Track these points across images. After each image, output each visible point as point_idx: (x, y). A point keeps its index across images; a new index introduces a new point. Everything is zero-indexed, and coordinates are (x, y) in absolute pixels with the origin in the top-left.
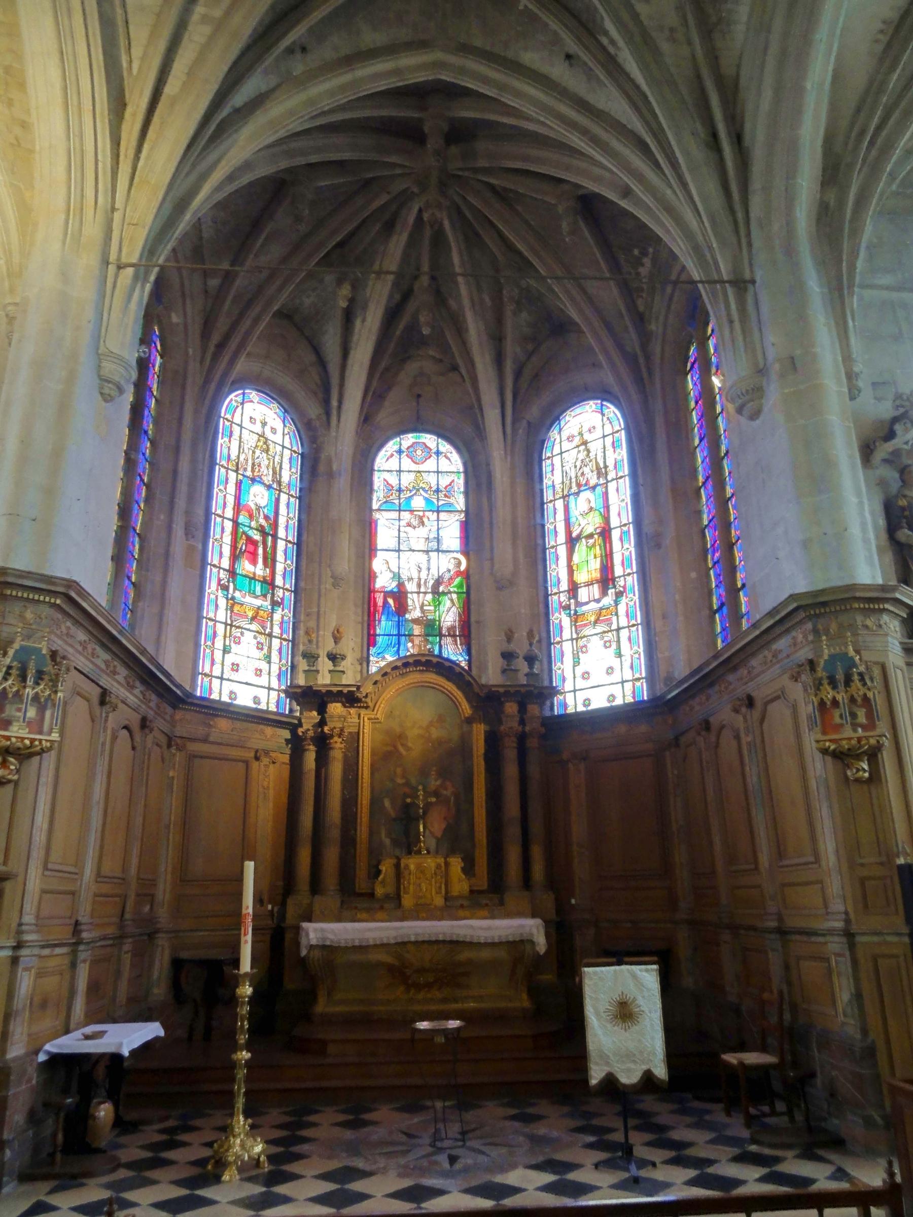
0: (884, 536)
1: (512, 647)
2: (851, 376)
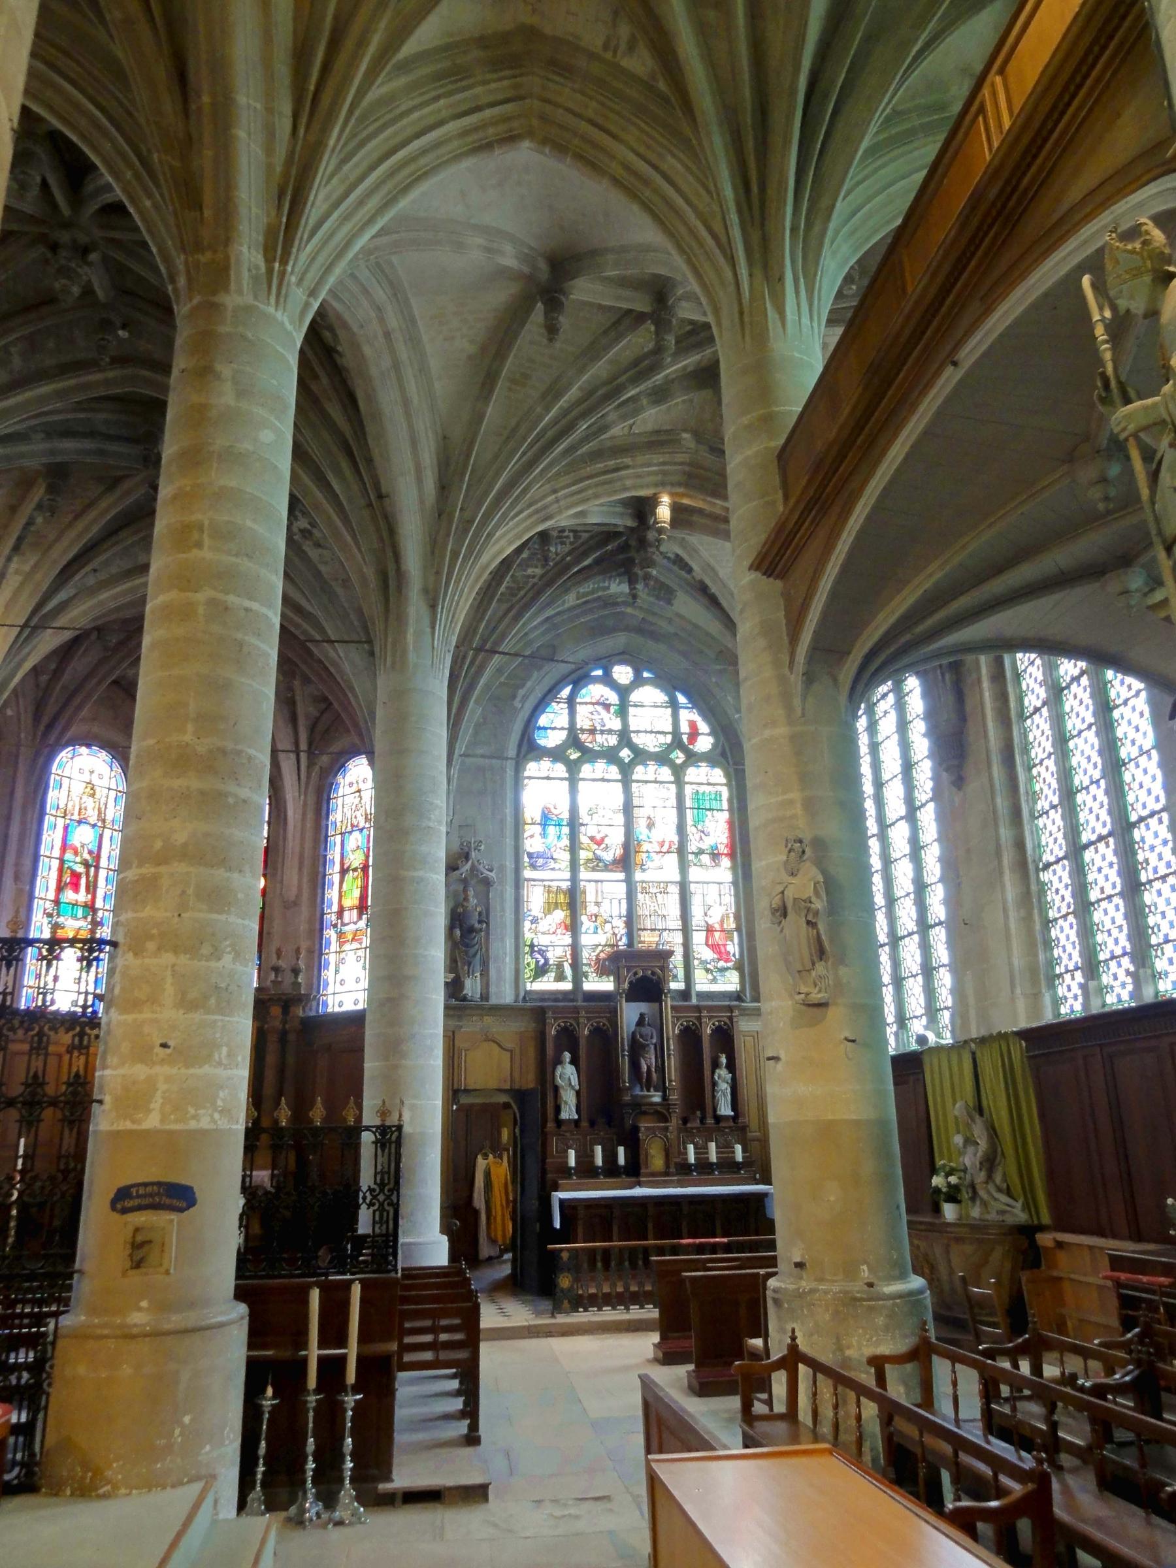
1: (281, 963)
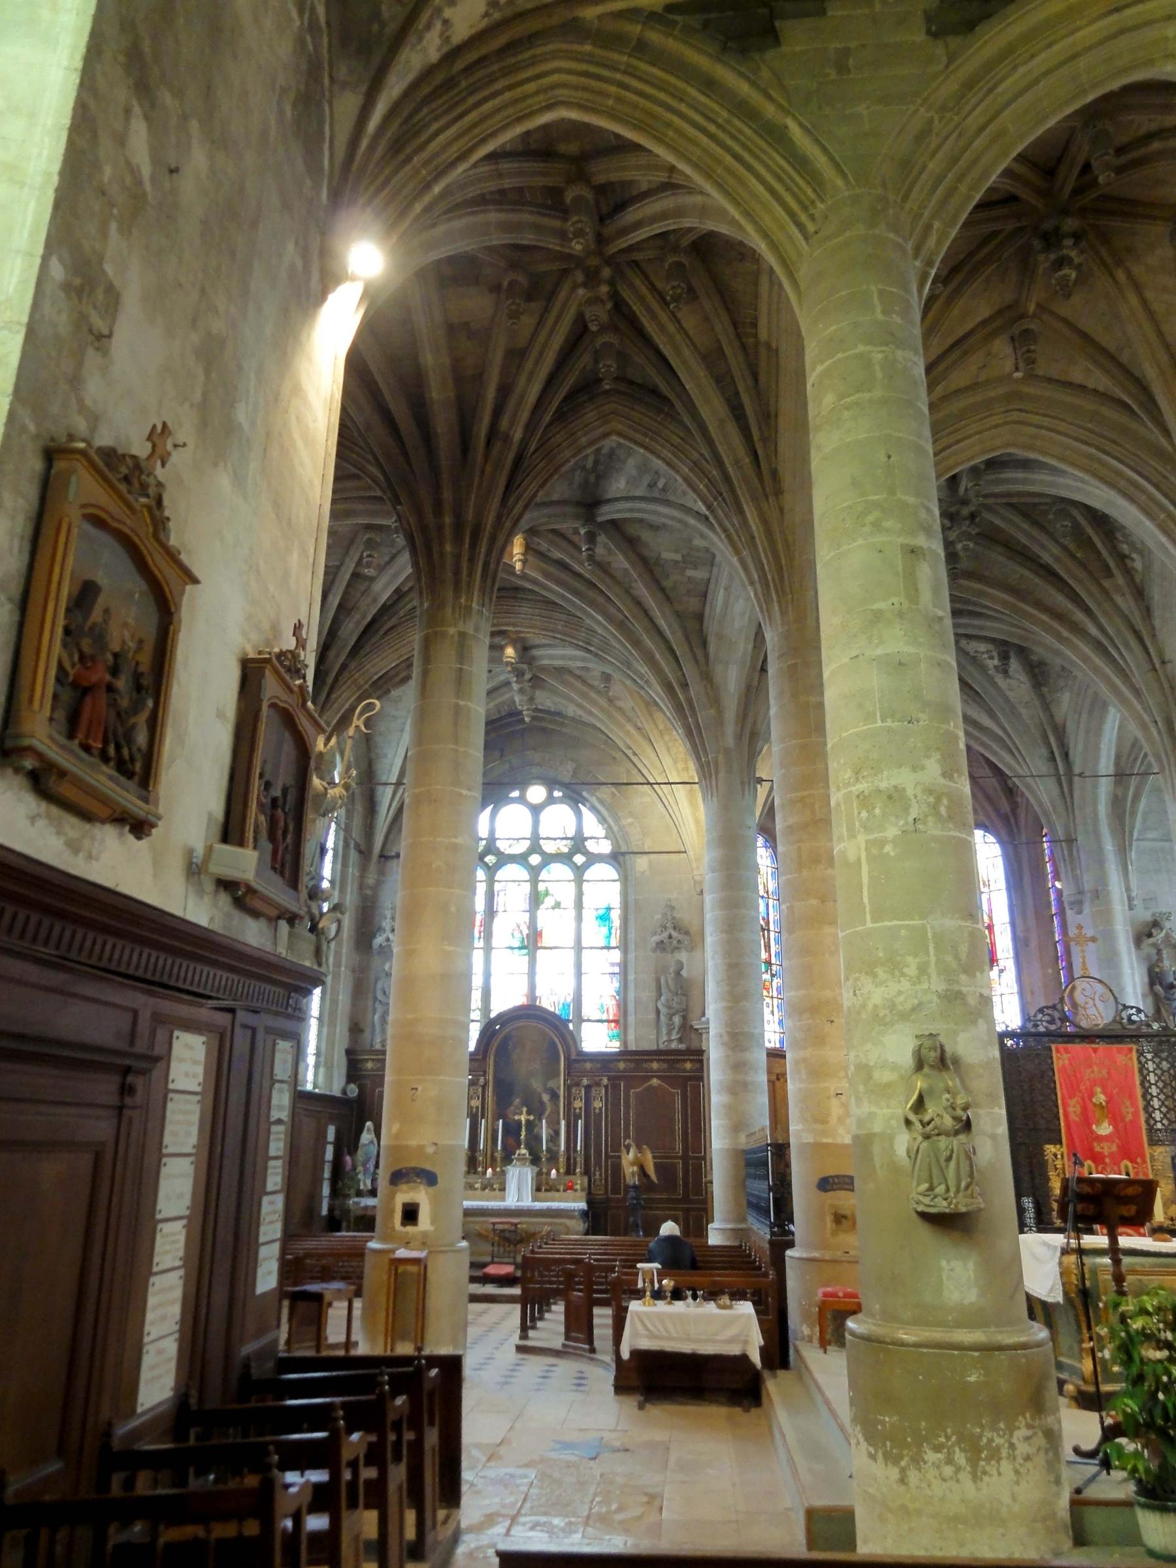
0: (1147, 987)
2: (1130, 899)
